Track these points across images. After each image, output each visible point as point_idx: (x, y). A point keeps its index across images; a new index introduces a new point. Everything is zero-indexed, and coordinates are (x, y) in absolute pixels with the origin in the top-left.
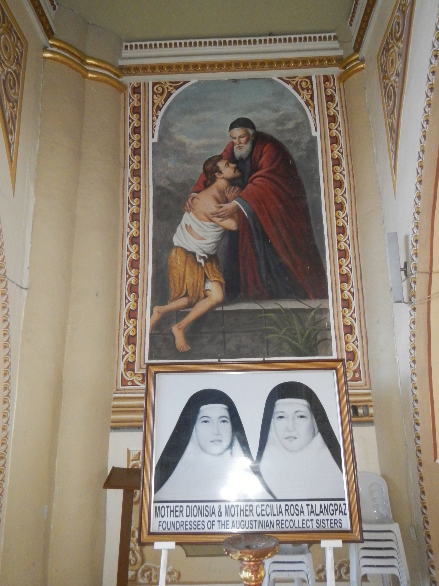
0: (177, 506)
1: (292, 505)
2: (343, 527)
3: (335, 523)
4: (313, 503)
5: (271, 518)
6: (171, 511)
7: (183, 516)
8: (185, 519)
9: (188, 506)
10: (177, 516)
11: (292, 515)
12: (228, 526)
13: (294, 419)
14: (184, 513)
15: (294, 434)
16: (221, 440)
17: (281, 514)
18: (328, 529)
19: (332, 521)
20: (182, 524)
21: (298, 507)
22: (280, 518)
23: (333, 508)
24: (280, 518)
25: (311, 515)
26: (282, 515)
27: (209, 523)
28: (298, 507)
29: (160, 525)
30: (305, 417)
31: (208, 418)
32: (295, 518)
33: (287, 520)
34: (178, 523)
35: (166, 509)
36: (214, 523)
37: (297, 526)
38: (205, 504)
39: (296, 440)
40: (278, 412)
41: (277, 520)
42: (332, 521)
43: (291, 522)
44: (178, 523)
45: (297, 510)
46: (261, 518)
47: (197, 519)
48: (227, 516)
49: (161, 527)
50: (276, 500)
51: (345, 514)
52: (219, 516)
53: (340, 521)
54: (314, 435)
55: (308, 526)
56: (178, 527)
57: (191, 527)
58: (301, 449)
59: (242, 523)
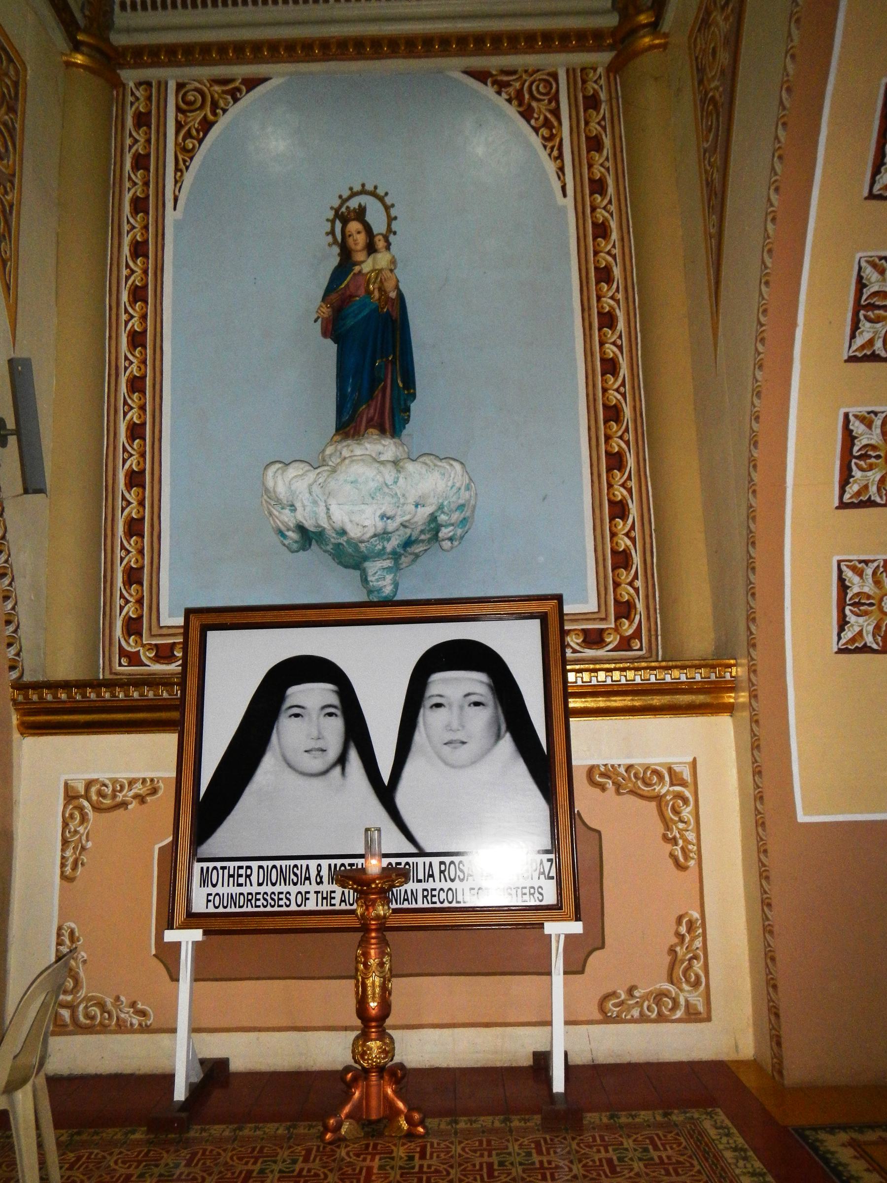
0: (240, 867)
1: (452, 862)
3: (530, 894)
6: (230, 876)
8: (255, 889)
9: (260, 867)
10: (240, 885)
11: (452, 880)
12: (333, 902)
13: (461, 708)
14: (254, 878)
15: (459, 736)
17: (431, 879)
20: (250, 898)
22: (430, 885)
24: (430, 885)
26: (434, 881)
27: (299, 896)
29: (208, 901)
30: (483, 705)
31: (302, 710)
33: (442, 889)
34: (242, 897)
35: (221, 872)
36: (308, 896)
38: (292, 863)
39: (465, 746)
40: (433, 696)
41: (424, 890)
43: (450, 892)
44: (242, 897)
47: (277, 889)
49: (211, 904)
50: (422, 854)
52: (318, 884)
53: (540, 890)
54: (498, 737)
56: (241, 904)
57: (265, 903)
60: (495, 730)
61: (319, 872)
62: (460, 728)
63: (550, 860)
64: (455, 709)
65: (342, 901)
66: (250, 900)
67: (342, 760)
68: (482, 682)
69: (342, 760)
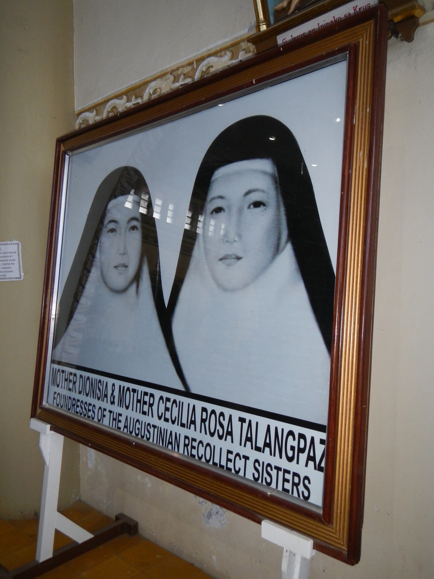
1: (213, 412)
2: (310, 501)
3: (294, 484)
4: (254, 418)
5: (176, 429)
7: (75, 392)
9: (81, 376)
11: (212, 435)
13: (240, 211)
15: (236, 249)
16: (127, 265)
18: (275, 494)
19: (287, 476)
21: (224, 420)
22: (191, 433)
23: (295, 444)
24: (191, 433)
25: (245, 446)
28: (224, 420)
29: (54, 398)
30: (264, 205)
32: (215, 441)
37: (217, 460)
39: (240, 262)
40: (214, 198)
42: (287, 476)
43: (208, 448)
45: (222, 425)
46: (161, 424)
48: (120, 406)
49: (55, 401)
50: (188, 394)
51: (320, 469)
53: (306, 482)
55: (237, 469)
58: (246, 285)
59: (138, 426)
60: (273, 240)
61: (113, 391)
62: (237, 239)
63: (322, 442)
64: (234, 210)
65: (126, 427)
66: (74, 405)
67: (137, 278)
68: (265, 173)
69: (137, 278)
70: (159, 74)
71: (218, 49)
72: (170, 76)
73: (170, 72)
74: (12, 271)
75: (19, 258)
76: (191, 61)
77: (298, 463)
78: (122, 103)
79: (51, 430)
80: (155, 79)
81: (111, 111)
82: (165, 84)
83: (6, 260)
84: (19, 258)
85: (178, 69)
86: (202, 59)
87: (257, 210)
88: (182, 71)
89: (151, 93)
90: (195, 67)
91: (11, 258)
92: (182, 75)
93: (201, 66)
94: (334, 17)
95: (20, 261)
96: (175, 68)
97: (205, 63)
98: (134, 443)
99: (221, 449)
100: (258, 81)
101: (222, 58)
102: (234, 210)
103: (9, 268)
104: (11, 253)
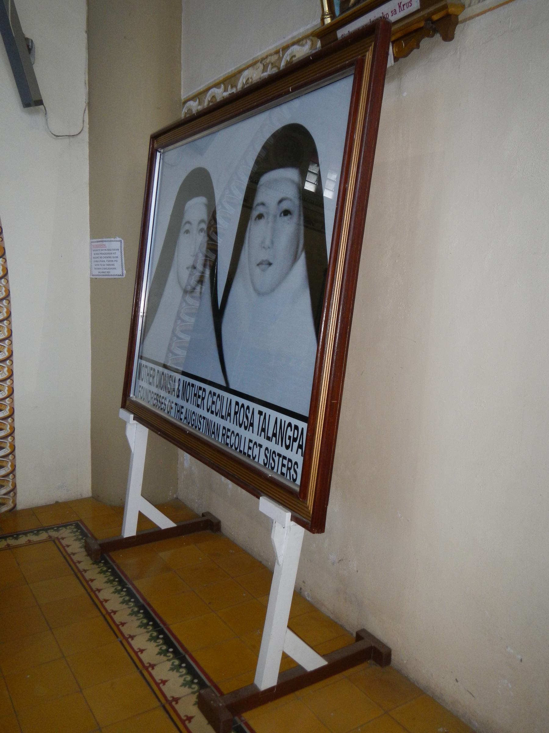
19: (285, 462)
28: (249, 413)
32: (241, 431)
37: (242, 449)
39: (271, 268)
40: (258, 205)
46: (209, 416)
50: (227, 389)
64: (271, 218)
65: (185, 418)
66: (152, 398)
68: (293, 181)
70: (251, 62)
71: (301, 37)
72: (260, 64)
73: (261, 60)
74: (115, 269)
75: (121, 255)
76: (278, 49)
77: (292, 451)
78: (220, 92)
79: (134, 420)
80: (247, 68)
81: (211, 101)
82: (256, 73)
83: (110, 257)
84: (121, 255)
85: (267, 57)
86: (286, 48)
87: (286, 218)
88: (270, 61)
89: (244, 83)
90: (281, 55)
91: (115, 255)
92: (269, 64)
93: (286, 55)
94: (383, 13)
95: (123, 258)
96: (264, 56)
97: (289, 52)
98: (188, 432)
99: (245, 438)
100: (293, 90)
101: (304, 47)
102: (271, 218)
103: (113, 265)
104: (114, 250)
